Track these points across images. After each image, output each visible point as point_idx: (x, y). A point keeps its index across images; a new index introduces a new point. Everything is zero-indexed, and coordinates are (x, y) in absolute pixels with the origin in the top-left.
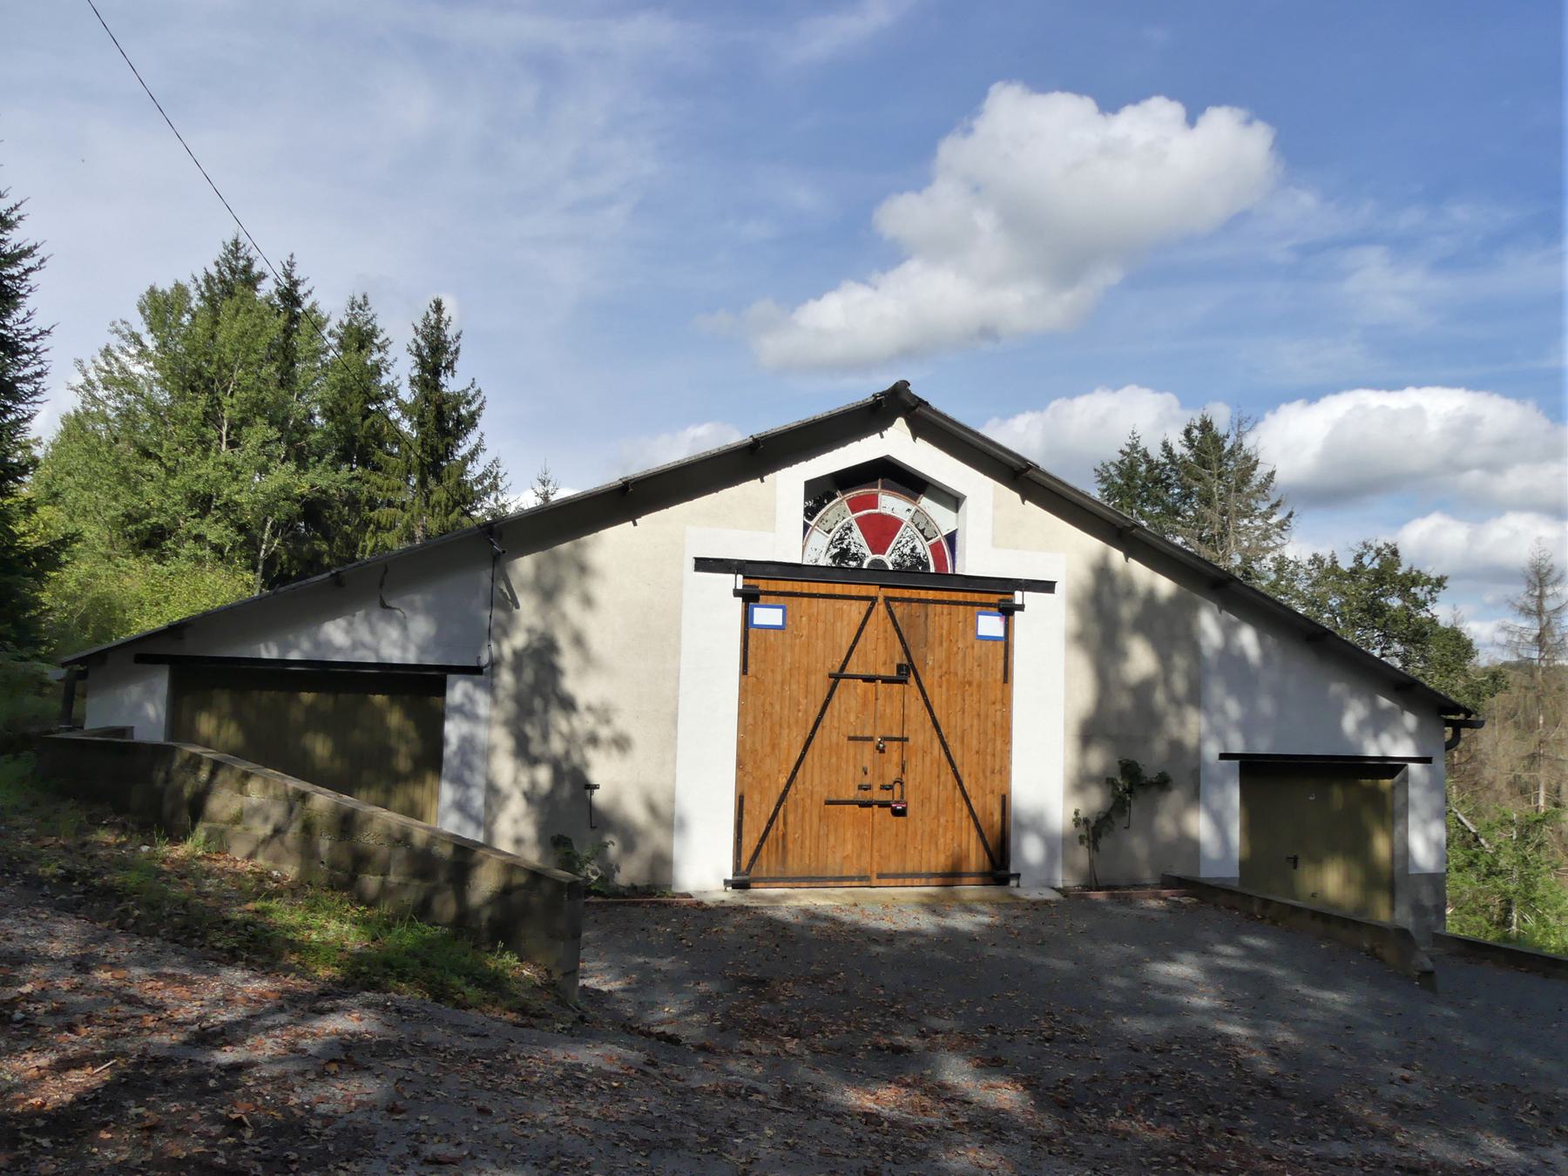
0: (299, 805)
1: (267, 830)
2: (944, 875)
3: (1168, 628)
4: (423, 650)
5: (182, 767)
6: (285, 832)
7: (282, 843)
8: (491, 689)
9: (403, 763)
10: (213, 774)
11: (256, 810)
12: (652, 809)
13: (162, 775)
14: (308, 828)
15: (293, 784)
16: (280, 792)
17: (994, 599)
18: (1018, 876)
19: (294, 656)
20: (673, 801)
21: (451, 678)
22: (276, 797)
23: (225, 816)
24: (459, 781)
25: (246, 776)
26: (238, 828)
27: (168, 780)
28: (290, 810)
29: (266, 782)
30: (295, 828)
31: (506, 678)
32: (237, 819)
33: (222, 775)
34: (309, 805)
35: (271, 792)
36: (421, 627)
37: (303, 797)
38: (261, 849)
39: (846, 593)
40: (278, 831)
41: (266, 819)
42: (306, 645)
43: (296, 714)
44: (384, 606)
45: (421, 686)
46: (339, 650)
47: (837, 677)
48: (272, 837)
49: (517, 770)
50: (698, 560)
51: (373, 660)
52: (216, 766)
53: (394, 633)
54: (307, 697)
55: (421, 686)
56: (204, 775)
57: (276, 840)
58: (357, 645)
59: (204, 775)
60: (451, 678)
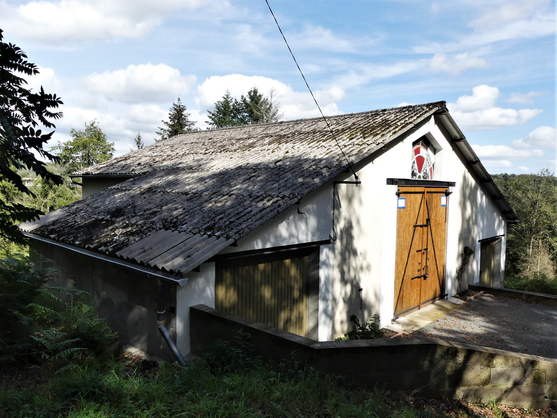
0: (530, 368)
1: (510, 384)
2: (431, 300)
3: (283, 171)
4: (313, 235)
5: (442, 357)
6: (521, 384)
7: (519, 390)
8: (333, 250)
9: (296, 294)
10: (467, 358)
11: (501, 375)
12: (376, 295)
13: (426, 363)
14: (538, 381)
15: (524, 357)
16: (516, 362)
17: (444, 190)
18: (447, 295)
19: (268, 246)
20: (380, 290)
21: (322, 247)
22: (514, 366)
23: (477, 381)
24: (325, 299)
25: (492, 356)
26: (488, 387)
27: (432, 364)
28: (525, 372)
29: (506, 358)
30: (529, 380)
31: (338, 244)
32: (487, 382)
33: (474, 358)
34: (537, 367)
35: (510, 363)
36: (313, 222)
37: (533, 363)
38: (504, 397)
39: (416, 191)
40: (516, 384)
41: (508, 379)
42: (272, 239)
43: (258, 277)
44: (299, 212)
45: (308, 254)
46: (284, 239)
47: (415, 227)
48: (512, 389)
49: (341, 288)
50: (388, 179)
51: (297, 243)
52: (470, 353)
53: (303, 226)
54: (261, 266)
55: (308, 254)
56: (460, 358)
57: (515, 389)
58: (291, 236)
59: (460, 358)
60: (322, 247)
